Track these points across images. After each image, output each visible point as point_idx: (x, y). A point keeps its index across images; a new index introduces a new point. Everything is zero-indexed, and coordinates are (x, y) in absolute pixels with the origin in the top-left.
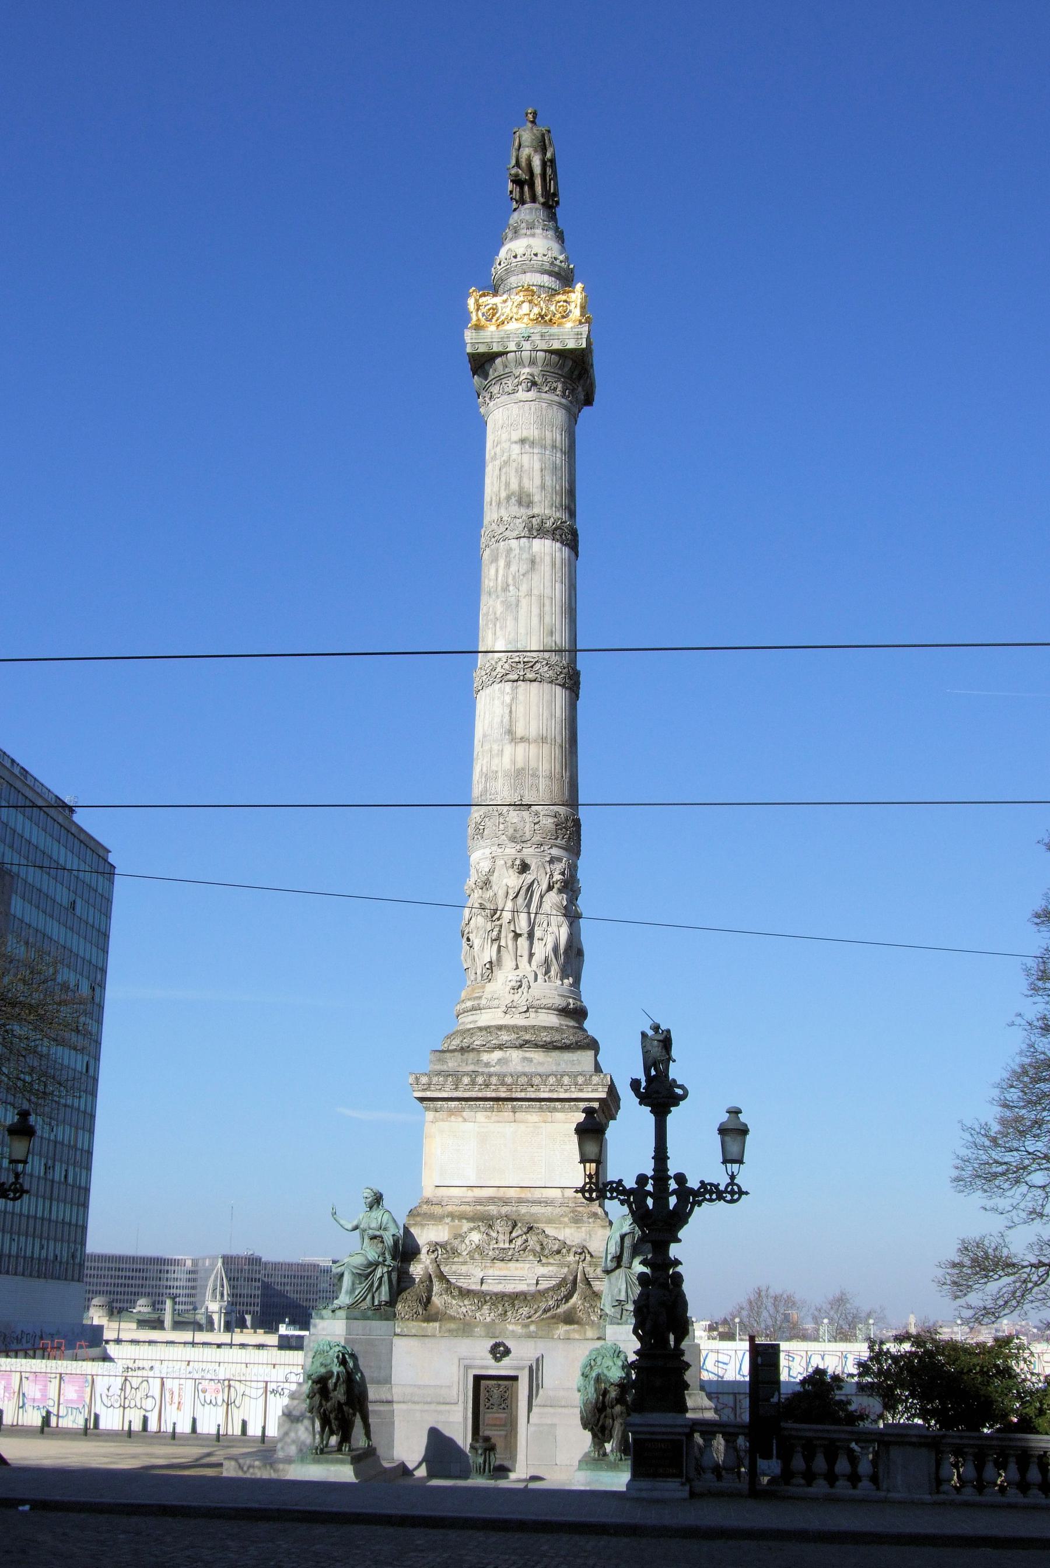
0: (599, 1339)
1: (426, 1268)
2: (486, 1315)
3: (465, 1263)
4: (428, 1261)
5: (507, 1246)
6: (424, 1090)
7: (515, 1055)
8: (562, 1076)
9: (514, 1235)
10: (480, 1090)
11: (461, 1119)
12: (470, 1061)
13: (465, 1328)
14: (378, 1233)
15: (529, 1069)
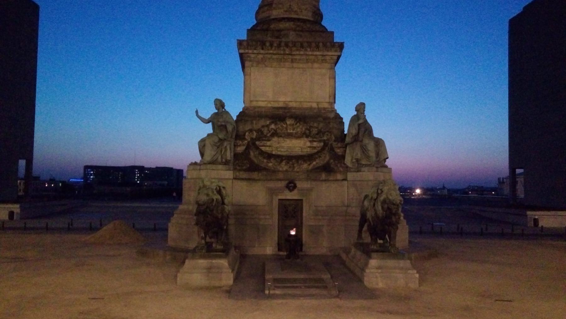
0: (343, 180)
1: (248, 142)
2: (284, 167)
3: (269, 140)
4: (249, 140)
5: (291, 131)
6: (244, 49)
7: (292, 33)
8: (319, 43)
9: (295, 126)
10: (275, 50)
11: (264, 65)
12: (268, 36)
13: (270, 173)
14: (223, 124)
15: (300, 40)
